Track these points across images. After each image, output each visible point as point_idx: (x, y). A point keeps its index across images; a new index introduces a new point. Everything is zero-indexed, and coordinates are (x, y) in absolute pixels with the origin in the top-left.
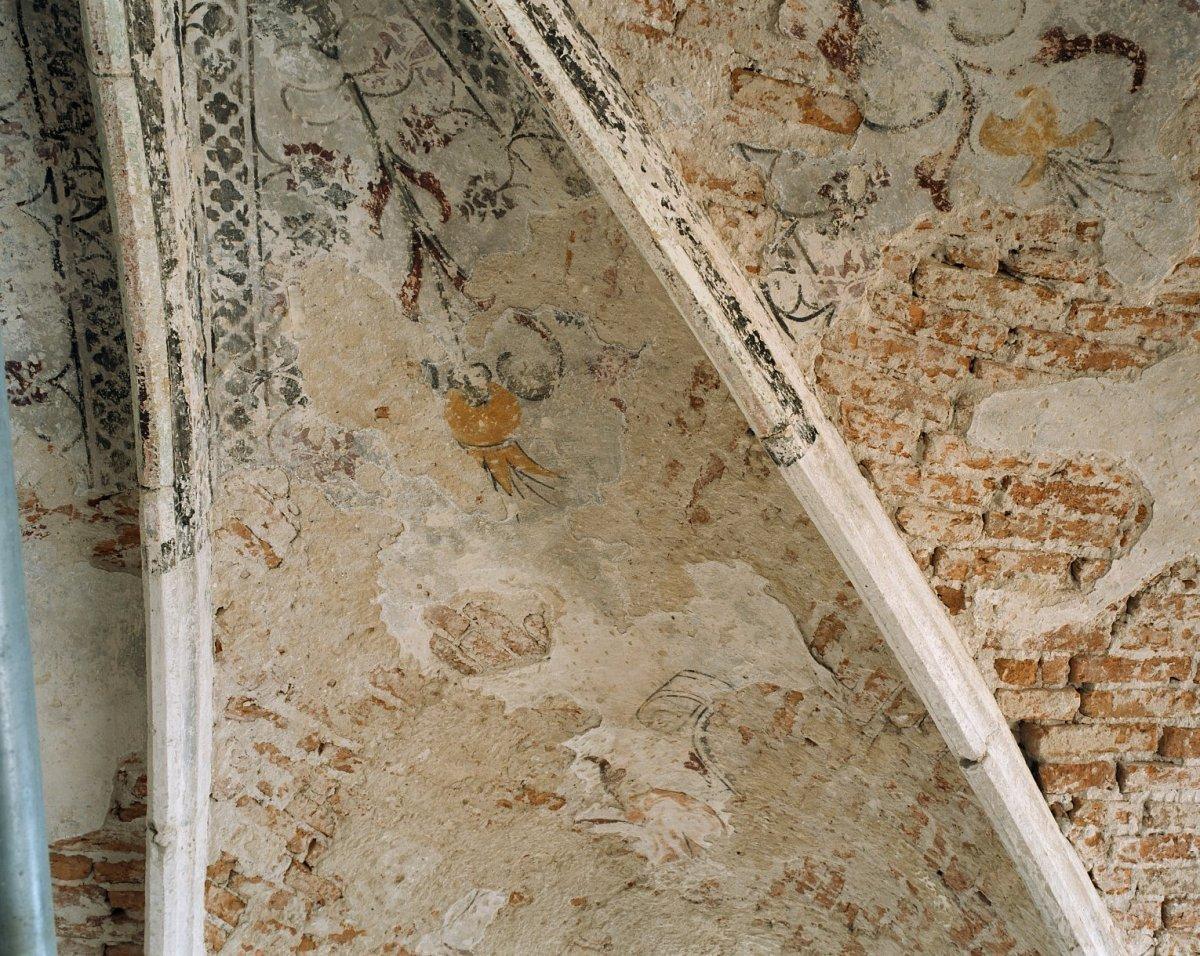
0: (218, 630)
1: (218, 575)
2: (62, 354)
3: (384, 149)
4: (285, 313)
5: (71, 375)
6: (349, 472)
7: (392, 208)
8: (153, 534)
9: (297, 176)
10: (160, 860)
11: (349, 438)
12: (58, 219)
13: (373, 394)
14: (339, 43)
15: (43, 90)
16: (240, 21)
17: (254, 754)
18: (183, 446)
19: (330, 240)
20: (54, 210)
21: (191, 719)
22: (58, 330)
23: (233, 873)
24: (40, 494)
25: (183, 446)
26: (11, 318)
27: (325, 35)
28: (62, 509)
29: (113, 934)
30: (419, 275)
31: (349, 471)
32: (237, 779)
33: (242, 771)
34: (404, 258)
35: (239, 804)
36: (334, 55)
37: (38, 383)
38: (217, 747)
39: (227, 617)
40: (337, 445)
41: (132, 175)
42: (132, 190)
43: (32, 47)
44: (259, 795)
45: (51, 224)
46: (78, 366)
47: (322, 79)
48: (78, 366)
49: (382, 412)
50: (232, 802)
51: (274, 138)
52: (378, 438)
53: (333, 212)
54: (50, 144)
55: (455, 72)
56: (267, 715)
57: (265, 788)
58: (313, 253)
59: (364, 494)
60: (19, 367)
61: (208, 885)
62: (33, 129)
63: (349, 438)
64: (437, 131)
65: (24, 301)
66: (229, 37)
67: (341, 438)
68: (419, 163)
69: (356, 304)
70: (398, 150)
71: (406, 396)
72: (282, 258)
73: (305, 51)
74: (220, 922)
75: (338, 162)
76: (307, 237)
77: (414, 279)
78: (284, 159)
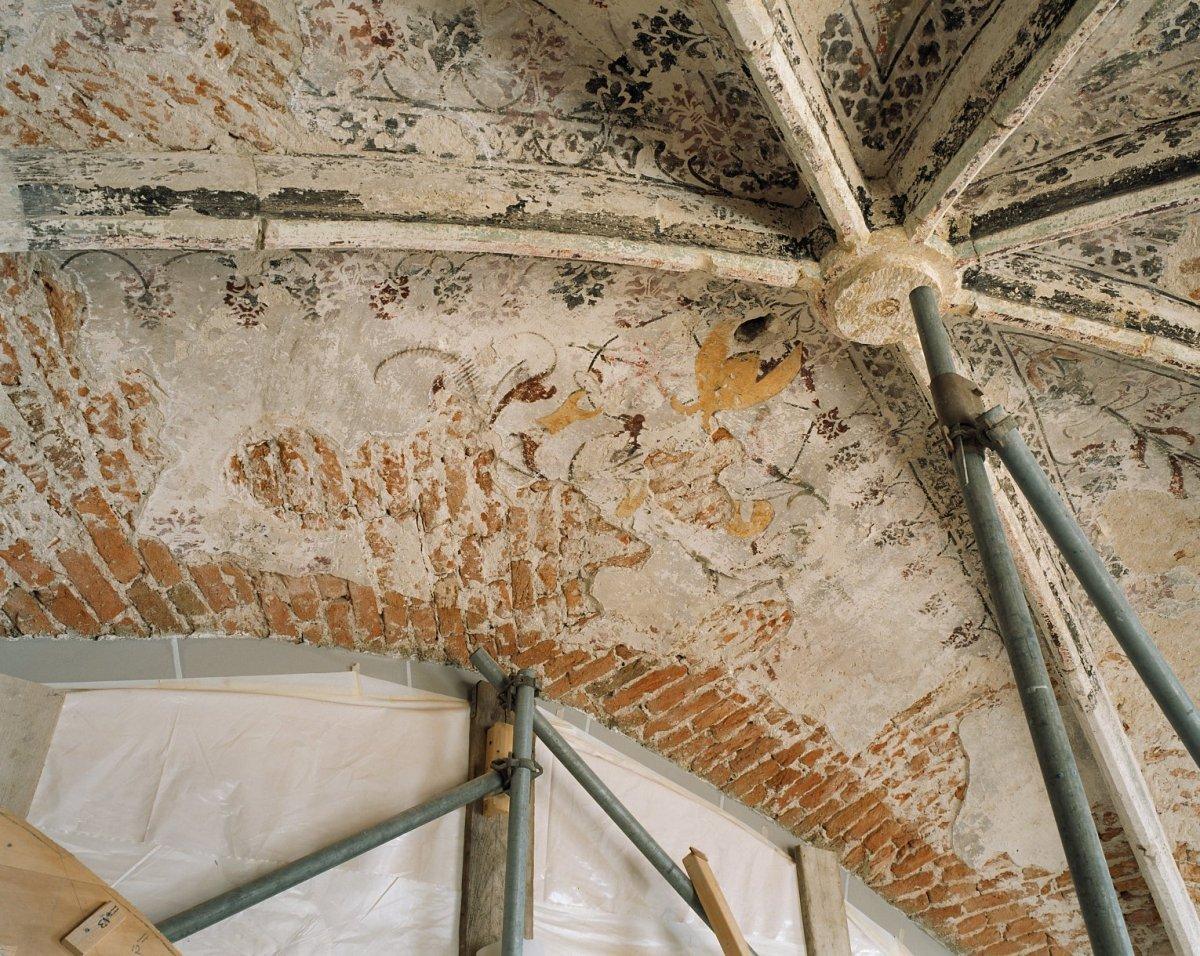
0: (1123, 718)
1: (1111, 687)
2: (980, 612)
3: (1136, 427)
4: (1099, 532)
5: (988, 620)
6: (1169, 596)
7: (1151, 451)
8: (1081, 692)
9: (1084, 465)
10: (1154, 864)
11: (1163, 578)
12: (960, 551)
13: (1170, 547)
14: (1094, 397)
15: (935, 499)
16: (1031, 415)
17: (1171, 778)
18: (1075, 636)
19: (1114, 484)
20: (956, 548)
21: (1135, 779)
22: (974, 602)
23: (1188, 852)
24: (990, 684)
25: (1075, 636)
26: (950, 608)
27: (1084, 397)
28: (1004, 687)
29: (1128, 908)
30: (1180, 474)
31: (1169, 595)
32: (1167, 796)
33: (1168, 791)
34: (1166, 471)
35: (1174, 810)
36: (1093, 402)
37: (974, 631)
38: (1149, 783)
39: (1125, 708)
40: (1156, 585)
41: (1013, 528)
42: (1016, 537)
43: (925, 484)
44: (1183, 800)
45: (957, 555)
46: (990, 613)
47: (1083, 415)
48: (990, 613)
49: (1180, 555)
50: (1170, 811)
51: (1063, 454)
52: (1183, 570)
53: (1111, 470)
54: (946, 520)
55: (1179, 380)
56: (1171, 753)
57: (1186, 795)
58: (1107, 495)
59: (1184, 603)
60: (961, 629)
61: (1178, 864)
62: (935, 518)
63: (1163, 578)
64: (1173, 408)
65: (954, 596)
66: (1026, 425)
67: (1158, 580)
68: (1163, 425)
69: (1141, 506)
70: (1147, 424)
71: (1193, 539)
72: (1088, 506)
73: (1073, 409)
74: (1193, 884)
75: (1107, 445)
76: (1099, 489)
77: (1177, 479)
78: (1074, 460)
